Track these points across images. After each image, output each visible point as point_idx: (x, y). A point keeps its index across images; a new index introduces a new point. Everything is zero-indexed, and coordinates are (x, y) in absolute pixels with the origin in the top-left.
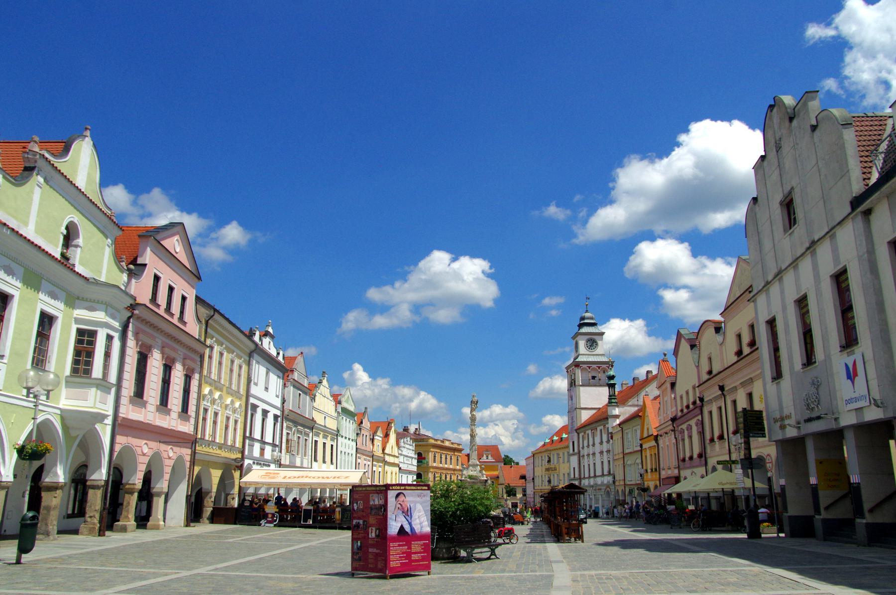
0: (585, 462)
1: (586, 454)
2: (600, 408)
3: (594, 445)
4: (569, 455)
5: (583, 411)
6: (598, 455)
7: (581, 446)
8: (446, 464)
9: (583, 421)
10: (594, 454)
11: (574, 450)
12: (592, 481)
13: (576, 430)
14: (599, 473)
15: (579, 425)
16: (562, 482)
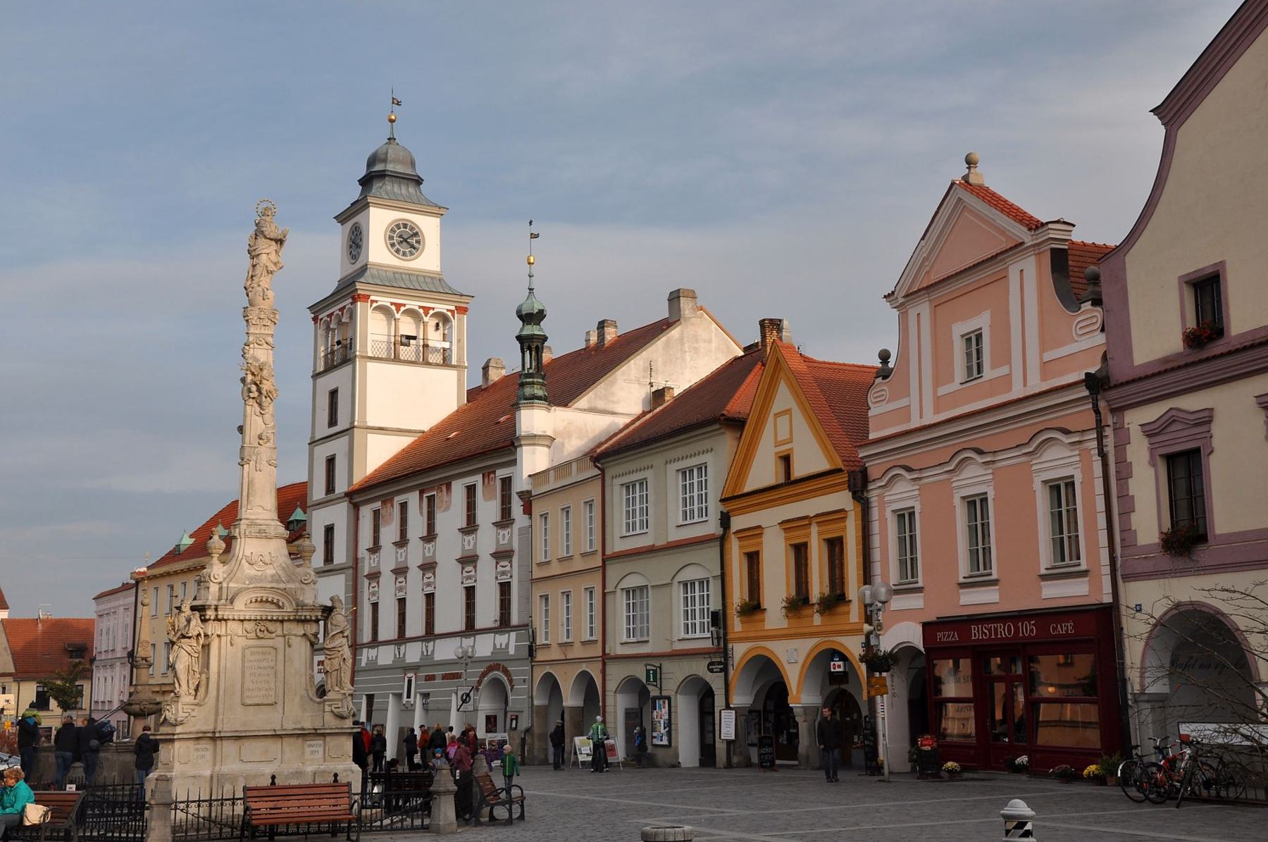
2: (424, 432)
3: (430, 537)
5: (373, 439)
7: (366, 541)
10: (428, 567)
11: (329, 557)
13: (350, 495)
14: (450, 616)
15: (358, 478)
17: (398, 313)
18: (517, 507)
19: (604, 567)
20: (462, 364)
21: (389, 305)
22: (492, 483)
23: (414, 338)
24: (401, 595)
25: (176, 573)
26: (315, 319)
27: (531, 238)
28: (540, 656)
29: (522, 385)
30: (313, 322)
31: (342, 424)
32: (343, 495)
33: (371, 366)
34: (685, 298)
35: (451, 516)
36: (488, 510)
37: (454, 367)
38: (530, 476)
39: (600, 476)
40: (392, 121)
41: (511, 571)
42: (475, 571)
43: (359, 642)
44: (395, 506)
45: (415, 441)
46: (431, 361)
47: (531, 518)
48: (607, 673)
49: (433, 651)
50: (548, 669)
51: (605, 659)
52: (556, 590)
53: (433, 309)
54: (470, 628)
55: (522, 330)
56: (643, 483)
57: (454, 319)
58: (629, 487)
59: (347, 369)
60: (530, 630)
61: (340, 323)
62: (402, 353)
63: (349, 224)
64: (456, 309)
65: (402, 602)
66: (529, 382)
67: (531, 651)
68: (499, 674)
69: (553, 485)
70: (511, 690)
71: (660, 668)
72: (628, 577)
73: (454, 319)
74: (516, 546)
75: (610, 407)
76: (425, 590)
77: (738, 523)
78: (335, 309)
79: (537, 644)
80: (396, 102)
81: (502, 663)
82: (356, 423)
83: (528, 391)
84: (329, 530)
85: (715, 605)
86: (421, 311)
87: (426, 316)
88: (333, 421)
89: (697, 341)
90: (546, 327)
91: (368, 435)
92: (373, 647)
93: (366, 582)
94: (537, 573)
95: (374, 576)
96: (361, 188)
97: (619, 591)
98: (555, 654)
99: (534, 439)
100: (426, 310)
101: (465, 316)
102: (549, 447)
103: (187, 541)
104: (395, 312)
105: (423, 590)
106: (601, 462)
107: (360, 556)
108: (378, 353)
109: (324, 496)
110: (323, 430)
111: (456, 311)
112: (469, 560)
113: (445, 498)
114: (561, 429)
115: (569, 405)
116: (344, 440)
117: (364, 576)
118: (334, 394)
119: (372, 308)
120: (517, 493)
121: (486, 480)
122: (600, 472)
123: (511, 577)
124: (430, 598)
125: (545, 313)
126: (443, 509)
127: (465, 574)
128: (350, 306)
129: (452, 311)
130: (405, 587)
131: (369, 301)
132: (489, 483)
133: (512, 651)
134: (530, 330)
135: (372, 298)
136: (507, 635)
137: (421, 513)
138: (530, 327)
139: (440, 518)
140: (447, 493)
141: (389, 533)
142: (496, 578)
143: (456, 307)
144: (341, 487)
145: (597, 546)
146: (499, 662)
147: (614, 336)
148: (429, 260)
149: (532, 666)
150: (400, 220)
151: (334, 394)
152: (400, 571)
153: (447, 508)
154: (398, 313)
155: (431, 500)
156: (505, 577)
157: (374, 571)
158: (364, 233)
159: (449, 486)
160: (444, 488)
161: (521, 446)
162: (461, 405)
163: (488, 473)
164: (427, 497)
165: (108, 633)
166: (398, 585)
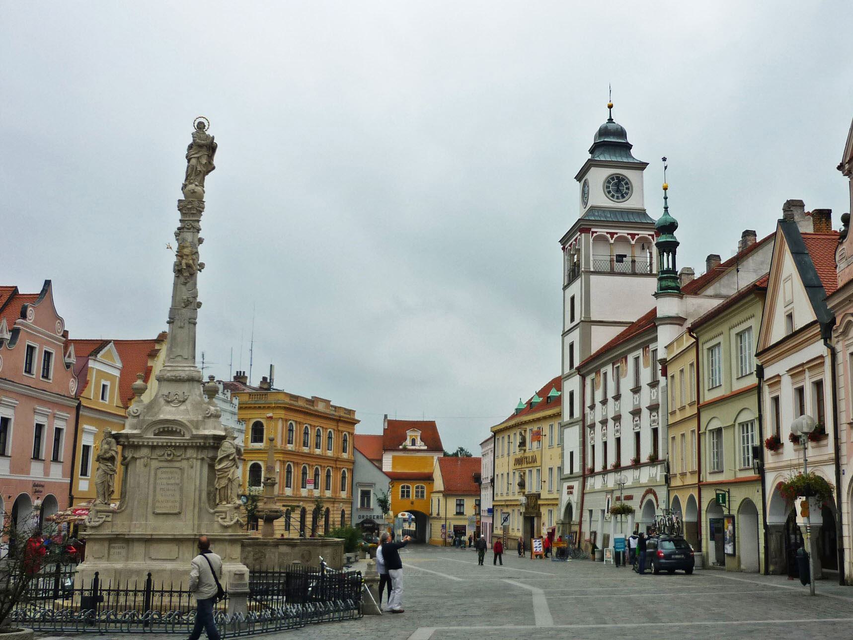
0: (597, 437)
1: (598, 418)
2: (633, 323)
3: (617, 397)
4: (563, 426)
5: (594, 328)
6: (627, 419)
7: (588, 403)
8: (305, 444)
9: (594, 351)
10: (617, 418)
12: (611, 480)
13: (579, 369)
16: (546, 486)
17: (612, 239)
19: (698, 415)
22: (647, 355)
23: (625, 256)
26: (563, 249)
28: (676, 482)
33: (593, 278)
35: (627, 383)
36: (646, 376)
38: (665, 347)
42: (640, 421)
45: (627, 329)
47: (667, 379)
48: (702, 496)
53: (638, 234)
62: (615, 267)
65: (605, 443)
66: (665, 277)
67: (667, 479)
70: (657, 508)
71: (729, 492)
72: (712, 422)
74: (660, 402)
76: (616, 435)
77: (769, 373)
79: (671, 474)
84: (572, 394)
86: (629, 237)
87: (633, 240)
88: (572, 319)
91: (592, 326)
95: (592, 426)
97: (707, 432)
100: (633, 236)
104: (610, 239)
107: (586, 412)
108: (618, 269)
111: (655, 236)
112: (636, 413)
113: (625, 368)
117: (588, 426)
119: (593, 237)
121: (644, 352)
123: (658, 423)
124: (618, 440)
126: (623, 376)
127: (635, 423)
128: (579, 237)
129: (652, 236)
135: (593, 230)
136: (656, 467)
141: (599, 396)
142: (651, 425)
143: (655, 232)
144: (577, 364)
145: (695, 399)
146: (651, 488)
149: (669, 491)
150: (614, 174)
152: (604, 422)
153: (626, 376)
154: (612, 239)
159: (626, 358)
163: (645, 346)
166: (603, 431)
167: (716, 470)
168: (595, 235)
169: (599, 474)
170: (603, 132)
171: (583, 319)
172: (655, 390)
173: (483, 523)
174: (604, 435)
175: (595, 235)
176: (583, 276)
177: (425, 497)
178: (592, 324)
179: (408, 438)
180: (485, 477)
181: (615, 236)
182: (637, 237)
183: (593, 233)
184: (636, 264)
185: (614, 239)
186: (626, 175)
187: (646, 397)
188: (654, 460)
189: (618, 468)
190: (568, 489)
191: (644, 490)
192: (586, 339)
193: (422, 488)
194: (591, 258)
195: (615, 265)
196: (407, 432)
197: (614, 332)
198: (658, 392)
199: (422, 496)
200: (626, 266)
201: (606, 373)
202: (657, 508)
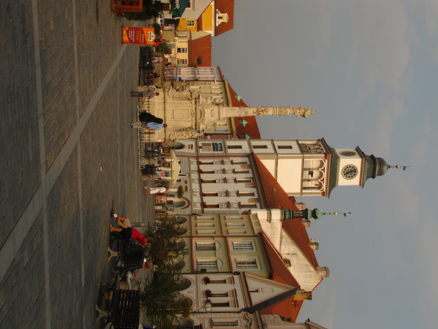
2: (276, 180)
3: (236, 181)
5: (273, 161)
7: (235, 160)
10: (225, 181)
11: (230, 147)
14: (207, 188)
15: (258, 156)
17: (321, 170)
18: (247, 209)
20: (303, 194)
21: (324, 166)
22: (255, 201)
23: (312, 176)
24: (215, 172)
25: (226, 95)
26: (319, 140)
27: (344, 214)
28: (193, 218)
29: (289, 211)
30: (318, 139)
31: (279, 151)
32: (252, 151)
33: (300, 161)
34: (325, 273)
36: (245, 201)
37: (302, 191)
39: (255, 235)
40: (397, 167)
41: (223, 208)
43: (199, 158)
44: (247, 169)
45: (274, 178)
46: (304, 182)
49: (195, 183)
50: (188, 220)
51: (191, 237)
52: (216, 222)
53: (323, 183)
54: (203, 195)
55: (310, 210)
56: (252, 249)
57: (321, 191)
58: (251, 244)
59: (298, 151)
60: (202, 214)
61: (317, 149)
63: (355, 152)
64: (324, 192)
65: (213, 172)
66: (291, 213)
68: (187, 204)
69: (253, 221)
70: (181, 208)
71: (188, 254)
72: (219, 245)
73: (321, 191)
74: (232, 209)
75: (283, 244)
77: (236, 277)
78: (322, 147)
79: (197, 217)
80: (405, 168)
81: (190, 205)
82: (279, 155)
83: (287, 213)
84: (240, 147)
85: (208, 270)
86: (322, 179)
87: (321, 180)
88: (280, 147)
89: (310, 277)
90: (311, 219)
92: (197, 163)
93: (221, 160)
94: (222, 217)
95: (222, 163)
96: (370, 155)
98: (193, 221)
99: (270, 215)
100: (323, 180)
101: (321, 195)
102: (267, 220)
103: (239, 98)
104: (321, 169)
105: (217, 179)
106: (260, 236)
107: (230, 158)
109: (252, 145)
110: (277, 144)
113: (250, 186)
114: (274, 225)
115: (283, 228)
116: (272, 151)
117: (223, 160)
118: (290, 147)
119: (322, 160)
120: (250, 210)
122: (256, 235)
123: (221, 208)
124: (214, 182)
125: (316, 219)
127: (222, 193)
128: (323, 152)
129: (323, 190)
130: (218, 173)
131: (325, 159)
132: (255, 200)
133: (195, 208)
134: (310, 214)
135: (326, 160)
137: (245, 178)
138: (311, 213)
139: (243, 184)
140: (252, 187)
141: (238, 168)
142: (220, 203)
143: (325, 192)
144: (256, 151)
145: (230, 235)
146: (191, 204)
147: (313, 248)
148: (342, 181)
149: (189, 215)
151: (290, 147)
152: (224, 171)
153: (246, 187)
154: (321, 170)
155: (250, 181)
156: (221, 206)
157: (225, 162)
158: (352, 157)
160: (254, 185)
161: (267, 210)
162: (287, 194)
163: (258, 200)
164: (250, 180)
165: (205, 72)
167: (197, 246)
168: (324, 161)
169: (199, 167)
170: (382, 162)
171: (279, 155)
172: (237, 206)
173: (173, 69)
174: (218, 172)
175: (324, 161)
176: (301, 155)
177: (188, 26)
178: (276, 160)
179: (223, 15)
180: (200, 70)
181: (323, 172)
182: (322, 182)
183: (325, 160)
184: (308, 182)
185: (321, 171)
186: (357, 176)
187: (234, 200)
188: (204, 205)
189: (201, 181)
190: (191, 145)
191: (189, 199)
192: (268, 156)
193: (193, 25)
194: (311, 159)
195: (307, 171)
196: (227, 14)
197: (272, 172)
198: (236, 208)
199: (188, 25)
200: (307, 175)
201: (249, 173)
202: (181, 208)
